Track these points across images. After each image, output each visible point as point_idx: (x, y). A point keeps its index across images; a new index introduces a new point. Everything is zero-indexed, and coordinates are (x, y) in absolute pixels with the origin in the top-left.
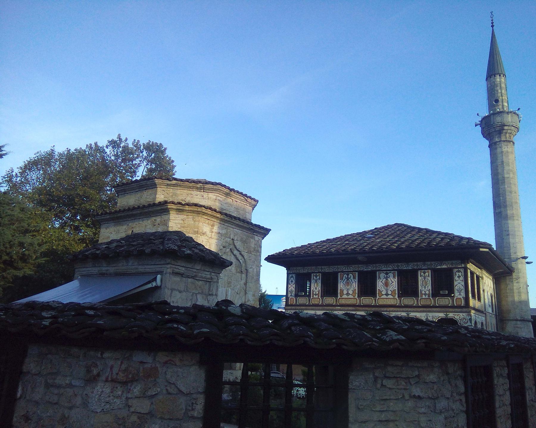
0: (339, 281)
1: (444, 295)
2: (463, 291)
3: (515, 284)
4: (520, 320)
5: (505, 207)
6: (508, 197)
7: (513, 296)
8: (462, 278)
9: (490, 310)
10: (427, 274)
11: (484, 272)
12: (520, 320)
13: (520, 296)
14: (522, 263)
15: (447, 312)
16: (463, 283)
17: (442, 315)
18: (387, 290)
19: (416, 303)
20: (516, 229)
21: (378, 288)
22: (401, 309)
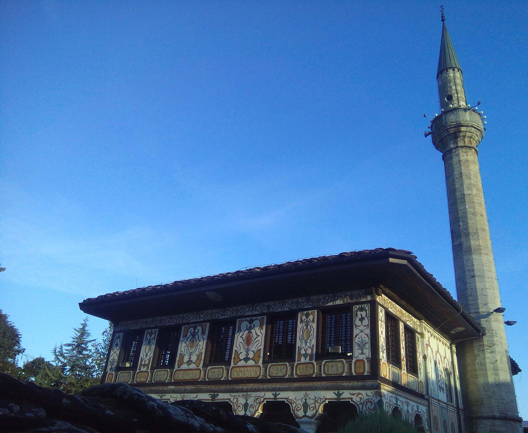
0: (182, 339)
1: (335, 356)
2: (368, 346)
3: (487, 355)
4: (499, 418)
5: (467, 235)
6: (470, 222)
7: (486, 375)
8: (366, 322)
9: (443, 397)
10: (311, 317)
11: (425, 324)
12: (499, 418)
13: (497, 374)
14: (497, 320)
15: (339, 388)
16: (368, 331)
17: (330, 395)
18: (247, 351)
19: (289, 373)
20: (485, 268)
21: (235, 348)
22: (265, 386)
